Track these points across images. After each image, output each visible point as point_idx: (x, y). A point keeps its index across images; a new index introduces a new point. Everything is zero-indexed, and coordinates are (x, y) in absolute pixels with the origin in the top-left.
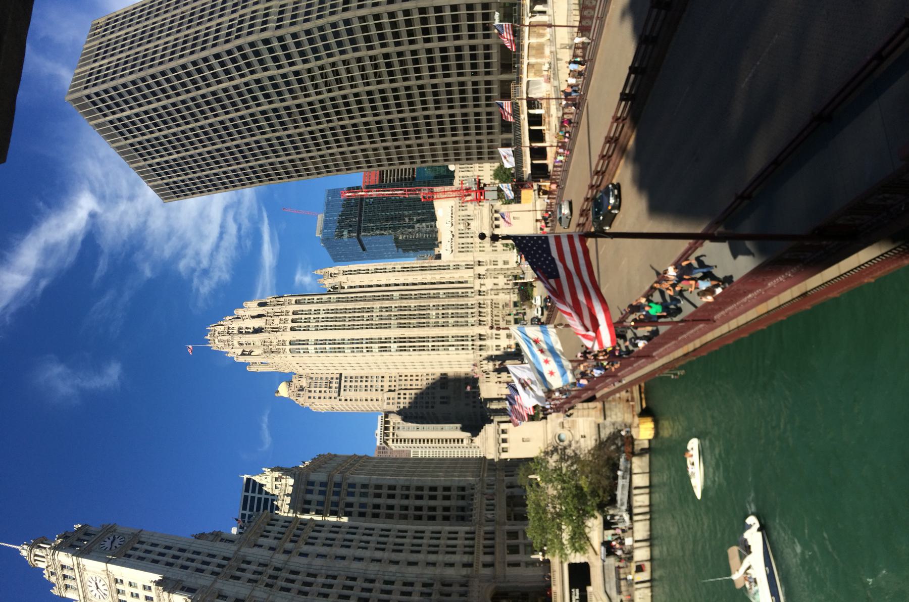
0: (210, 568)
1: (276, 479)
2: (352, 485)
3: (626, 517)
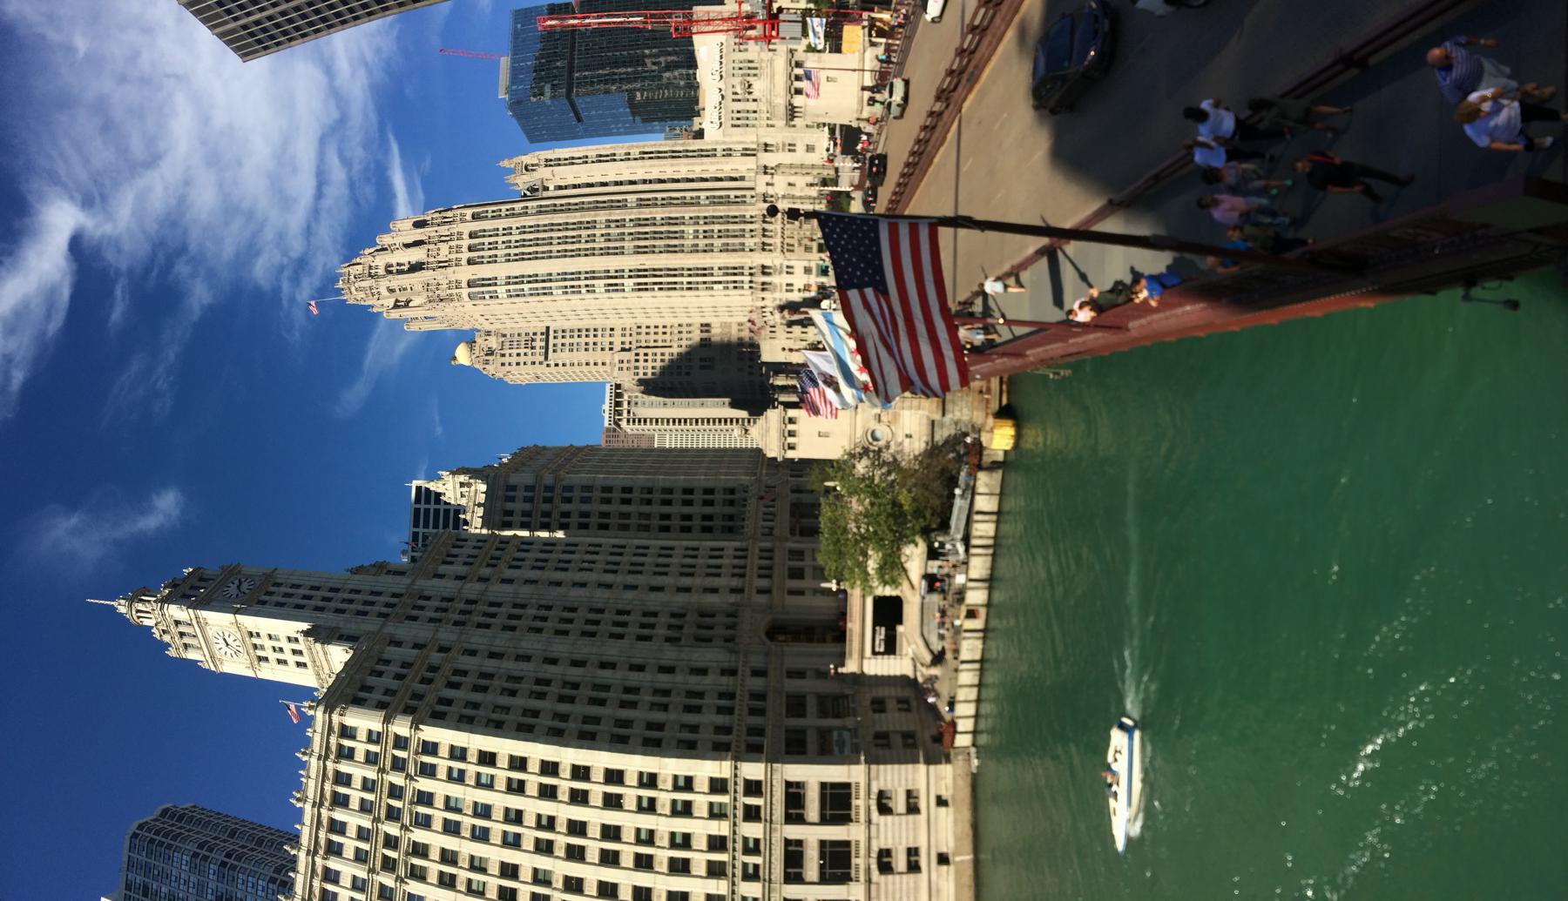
1: (462, 485)
2: (570, 488)
3: (961, 548)
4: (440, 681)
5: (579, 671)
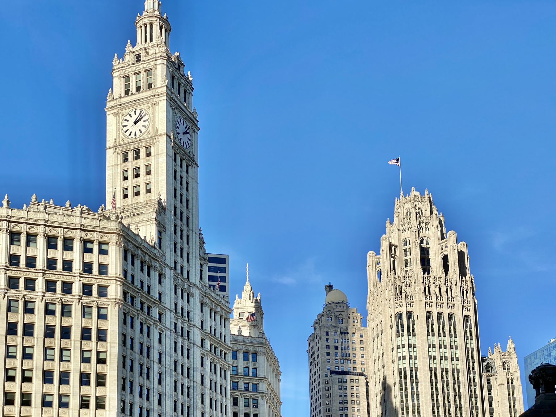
2: (256, 406)
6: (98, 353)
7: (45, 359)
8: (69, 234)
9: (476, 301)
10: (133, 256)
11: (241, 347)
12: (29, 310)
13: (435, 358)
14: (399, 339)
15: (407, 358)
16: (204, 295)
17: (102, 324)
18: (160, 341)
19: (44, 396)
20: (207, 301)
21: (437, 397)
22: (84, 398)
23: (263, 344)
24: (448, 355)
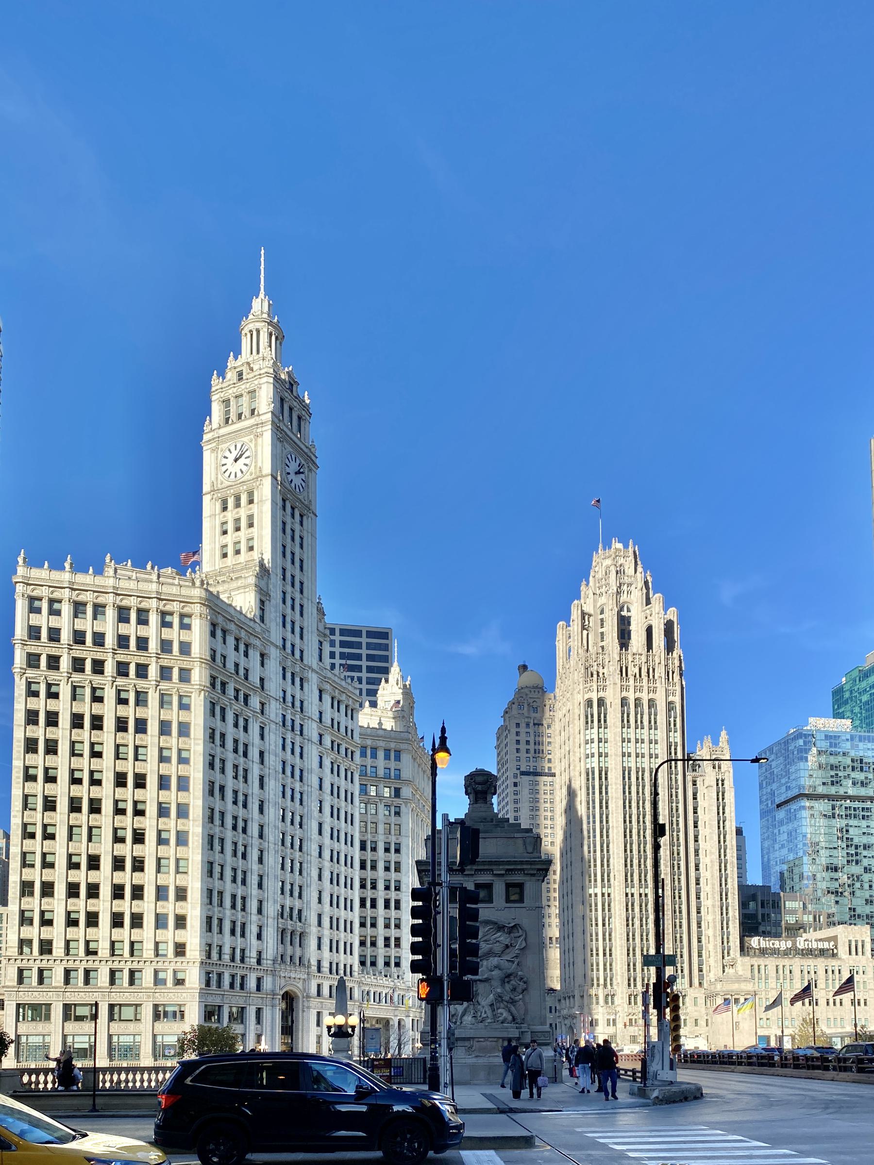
0: (289, 635)
4: (238, 706)
5: (256, 833)
6: (180, 751)
7: (117, 757)
8: (144, 605)
9: (684, 683)
10: (224, 632)
11: (381, 744)
12: (97, 699)
13: (629, 756)
14: (588, 732)
15: (596, 755)
16: (324, 679)
17: (184, 716)
18: (262, 737)
19: (116, 802)
20: (327, 687)
21: (630, 803)
22: (163, 805)
23: (408, 739)
24: (646, 752)
